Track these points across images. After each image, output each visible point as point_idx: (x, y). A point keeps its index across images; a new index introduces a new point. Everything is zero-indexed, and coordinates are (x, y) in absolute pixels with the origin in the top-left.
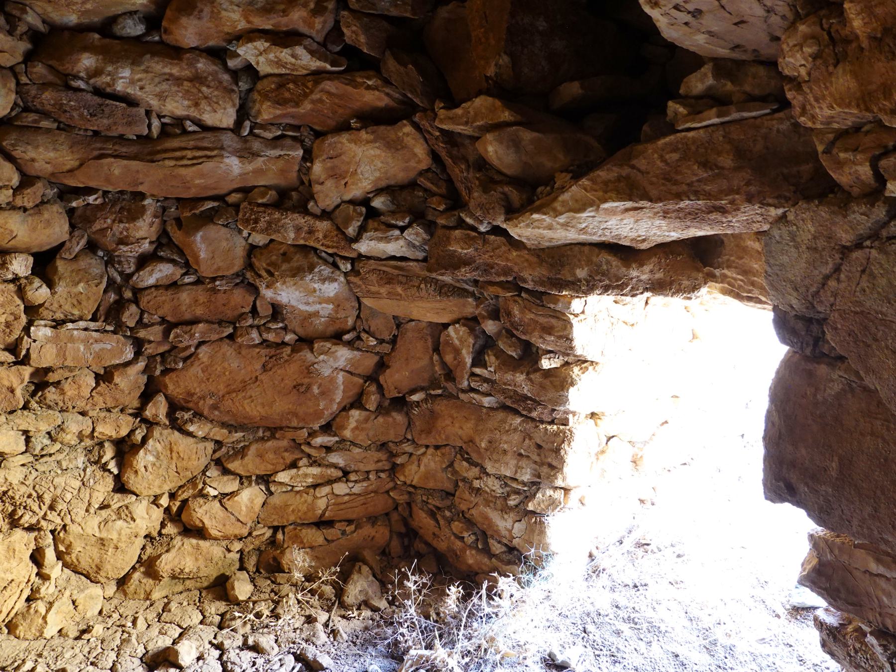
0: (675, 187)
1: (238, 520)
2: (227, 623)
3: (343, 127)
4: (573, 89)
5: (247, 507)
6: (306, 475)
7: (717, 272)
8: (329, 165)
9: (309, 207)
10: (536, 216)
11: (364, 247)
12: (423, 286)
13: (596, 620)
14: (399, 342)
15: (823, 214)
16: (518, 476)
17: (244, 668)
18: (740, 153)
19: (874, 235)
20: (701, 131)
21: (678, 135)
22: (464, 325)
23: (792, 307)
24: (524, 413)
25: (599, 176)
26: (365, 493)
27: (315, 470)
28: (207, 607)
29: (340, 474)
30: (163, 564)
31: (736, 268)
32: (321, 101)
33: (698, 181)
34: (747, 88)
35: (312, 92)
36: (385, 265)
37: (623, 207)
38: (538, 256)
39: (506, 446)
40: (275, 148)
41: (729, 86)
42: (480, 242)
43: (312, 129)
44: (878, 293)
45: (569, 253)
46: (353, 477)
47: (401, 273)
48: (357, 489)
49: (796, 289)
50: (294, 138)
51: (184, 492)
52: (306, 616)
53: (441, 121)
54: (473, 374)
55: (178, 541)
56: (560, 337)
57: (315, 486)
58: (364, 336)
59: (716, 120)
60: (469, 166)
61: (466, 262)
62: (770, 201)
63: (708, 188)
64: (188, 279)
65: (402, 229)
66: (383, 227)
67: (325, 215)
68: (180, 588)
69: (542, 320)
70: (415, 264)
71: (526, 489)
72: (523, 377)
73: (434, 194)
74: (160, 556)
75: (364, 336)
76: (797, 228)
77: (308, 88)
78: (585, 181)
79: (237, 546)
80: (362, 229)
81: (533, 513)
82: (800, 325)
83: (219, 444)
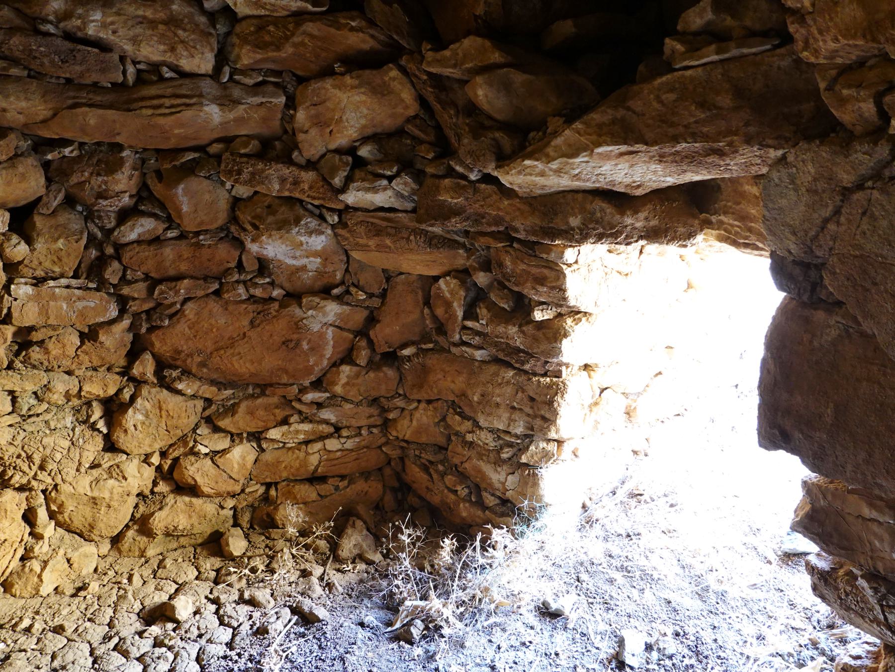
0: (670, 130)
1: (231, 477)
2: (223, 578)
3: (327, 72)
4: (566, 28)
5: (239, 464)
6: (297, 432)
7: (714, 219)
8: (313, 112)
9: (293, 156)
10: (527, 162)
11: (351, 198)
12: (412, 238)
13: (589, 570)
14: (389, 296)
15: (824, 154)
16: (511, 429)
17: (241, 621)
18: (739, 92)
19: (877, 175)
20: (700, 70)
21: (676, 73)
22: (455, 278)
23: (790, 252)
24: (517, 365)
25: (593, 119)
26: (358, 448)
27: (306, 427)
28: (202, 563)
29: (332, 430)
30: (156, 522)
31: (733, 213)
32: (302, 44)
33: (696, 122)
34: (748, 23)
35: (293, 35)
36: (373, 217)
37: (617, 151)
38: (531, 205)
39: (498, 399)
40: (255, 94)
41: (729, 21)
42: (471, 191)
43: (294, 75)
44: (879, 235)
45: (562, 200)
46: (345, 433)
47: (389, 224)
48: (349, 444)
49: (794, 233)
50: (276, 84)
51: (174, 450)
52: (301, 570)
53: (429, 64)
54: (465, 328)
55: (170, 499)
56: (553, 288)
57: (307, 443)
58: (353, 290)
59: (715, 58)
60: (458, 112)
61: (456, 212)
62: (770, 142)
63: (705, 130)
64: (170, 234)
65: (390, 179)
66: (370, 177)
67: (310, 165)
68: (175, 545)
69: (534, 271)
70: (404, 215)
71: (519, 441)
72: (515, 329)
73: (422, 142)
74: (153, 514)
75: (353, 290)
76: (797, 169)
77: (289, 30)
78: (578, 125)
79: (230, 503)
80: (349, 180)
81: (526, 465)
82: (797, 271)
83: (208, 402)
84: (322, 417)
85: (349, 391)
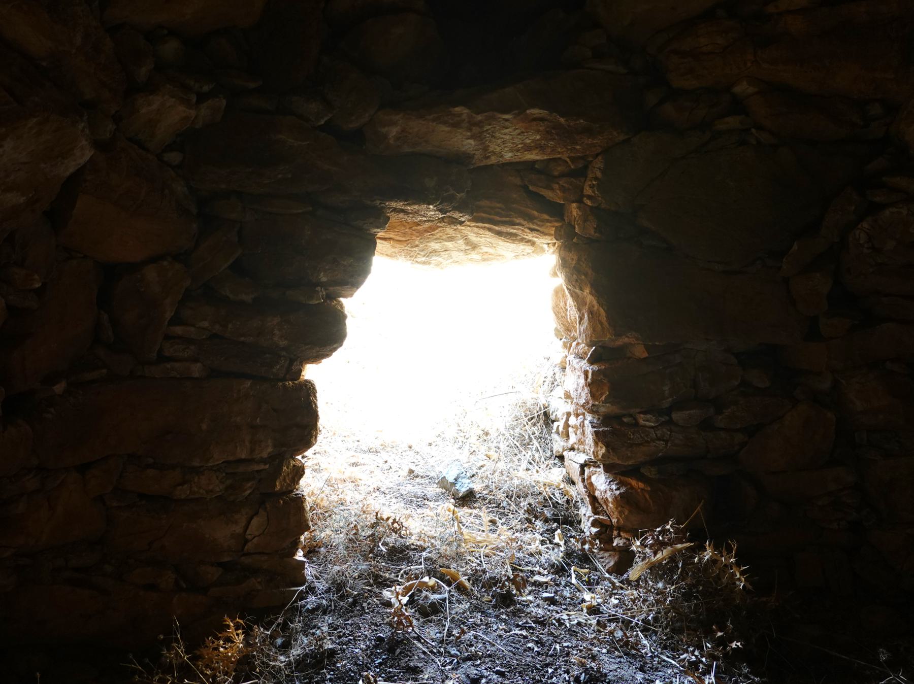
54: (167, 337)
71: (267, 466)
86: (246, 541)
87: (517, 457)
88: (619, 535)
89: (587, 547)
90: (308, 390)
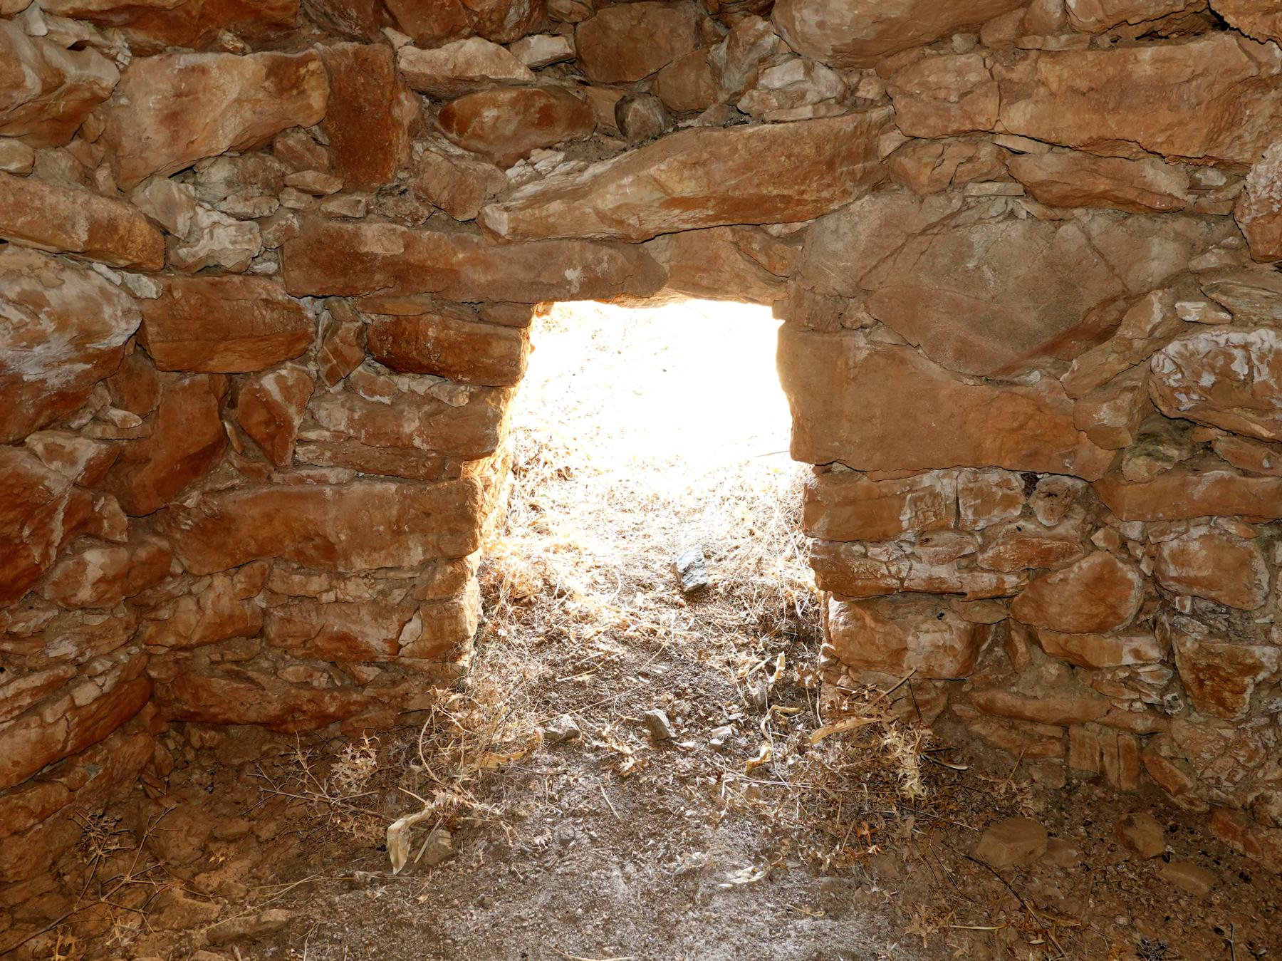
26: (119, 684)
29: (72, 670)
48: (109, 682)
57: (33, 709)
84: (53, 654)
85: (105, 592)
86: (401, 646)
87: (786, 538)
88: (847, 673)
89: (808, 679)
90: (468, 492)
